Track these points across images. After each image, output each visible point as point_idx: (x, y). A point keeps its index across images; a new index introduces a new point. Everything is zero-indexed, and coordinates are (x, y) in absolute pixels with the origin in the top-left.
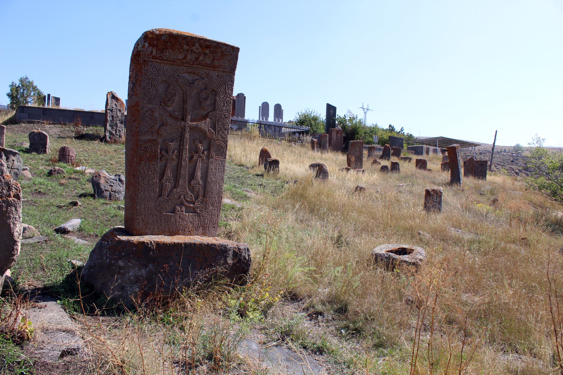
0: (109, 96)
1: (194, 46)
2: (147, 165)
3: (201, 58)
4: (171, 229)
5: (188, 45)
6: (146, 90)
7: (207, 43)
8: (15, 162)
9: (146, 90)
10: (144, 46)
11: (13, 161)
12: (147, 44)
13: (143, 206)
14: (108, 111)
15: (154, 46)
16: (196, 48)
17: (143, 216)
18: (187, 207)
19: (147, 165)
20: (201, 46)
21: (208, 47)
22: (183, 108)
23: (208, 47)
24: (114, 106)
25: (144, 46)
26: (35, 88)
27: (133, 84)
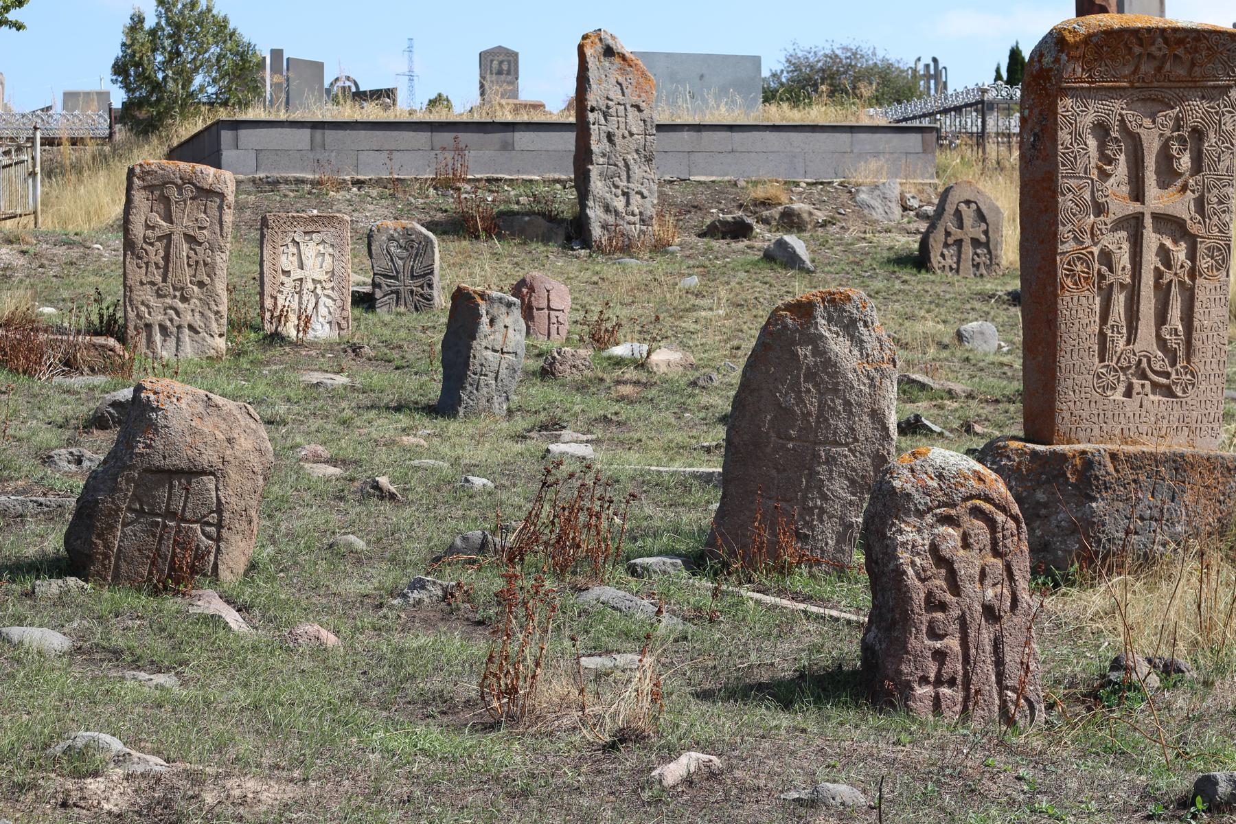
0: (589, 51)
1: (1153, 44)
2: (1076, 299)
3: (1168, 66)
4: (1126, 431)
5: (1141, 45)
6: (1067, 148)
7: (1178, 35)
8: (511, 331)
9: (1067, 148)
10: (1057, 60)
11: (506, 327)
12: (1064, 57)
13: (1070, 382)
14: (591, 117)
15: (1077, 59)
16: (1159, 48)
17: (1071, 404)
18: (1155, 385)
19: (1076, 299)
20: (1166, 41)
21: (1181, 42)
22: (1137, 175)
23: (1181, 42)
24: (615, 94)
25: (1057, 60)
26: (221, 29)
27: (1035, 135)
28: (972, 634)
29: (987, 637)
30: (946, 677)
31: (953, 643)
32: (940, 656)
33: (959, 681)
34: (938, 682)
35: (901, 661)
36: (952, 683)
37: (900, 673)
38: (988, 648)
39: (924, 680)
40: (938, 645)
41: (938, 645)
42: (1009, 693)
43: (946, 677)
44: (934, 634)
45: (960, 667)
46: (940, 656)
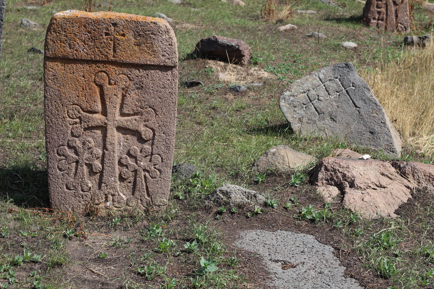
28: (389, 8)
29: (393, 9)
30: (380, 18)
31: (383, 10)
32: (379, 13)
33: (385, 19)
34: (378, 19)
35: (368, 13)
36: (382, 20)
37: (368, 16)
38: (394, 12)
39: (374, 19)
40: (379, 10)
41: (379, 10)
42: (399, 24)
43: (380, 18)
44: (378, 7)
45: (385, 16)
46: (379, 13)
